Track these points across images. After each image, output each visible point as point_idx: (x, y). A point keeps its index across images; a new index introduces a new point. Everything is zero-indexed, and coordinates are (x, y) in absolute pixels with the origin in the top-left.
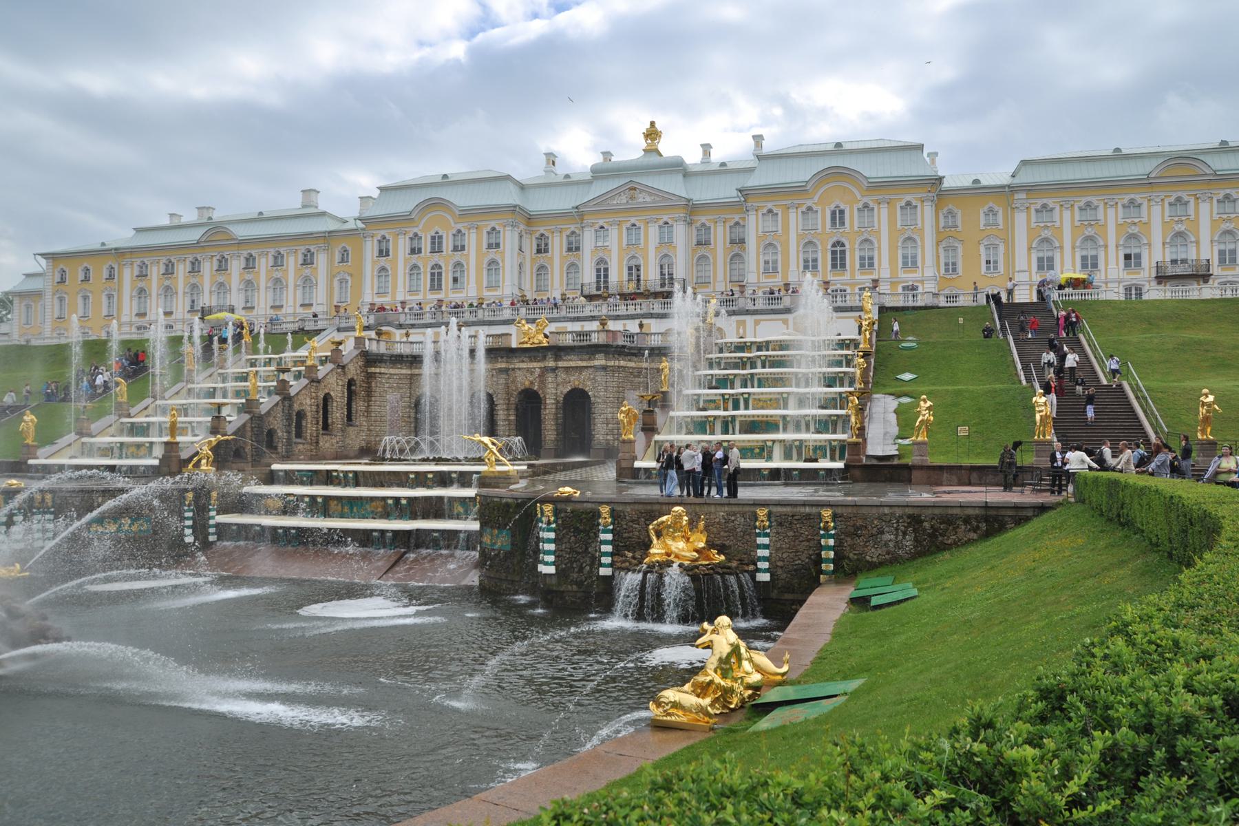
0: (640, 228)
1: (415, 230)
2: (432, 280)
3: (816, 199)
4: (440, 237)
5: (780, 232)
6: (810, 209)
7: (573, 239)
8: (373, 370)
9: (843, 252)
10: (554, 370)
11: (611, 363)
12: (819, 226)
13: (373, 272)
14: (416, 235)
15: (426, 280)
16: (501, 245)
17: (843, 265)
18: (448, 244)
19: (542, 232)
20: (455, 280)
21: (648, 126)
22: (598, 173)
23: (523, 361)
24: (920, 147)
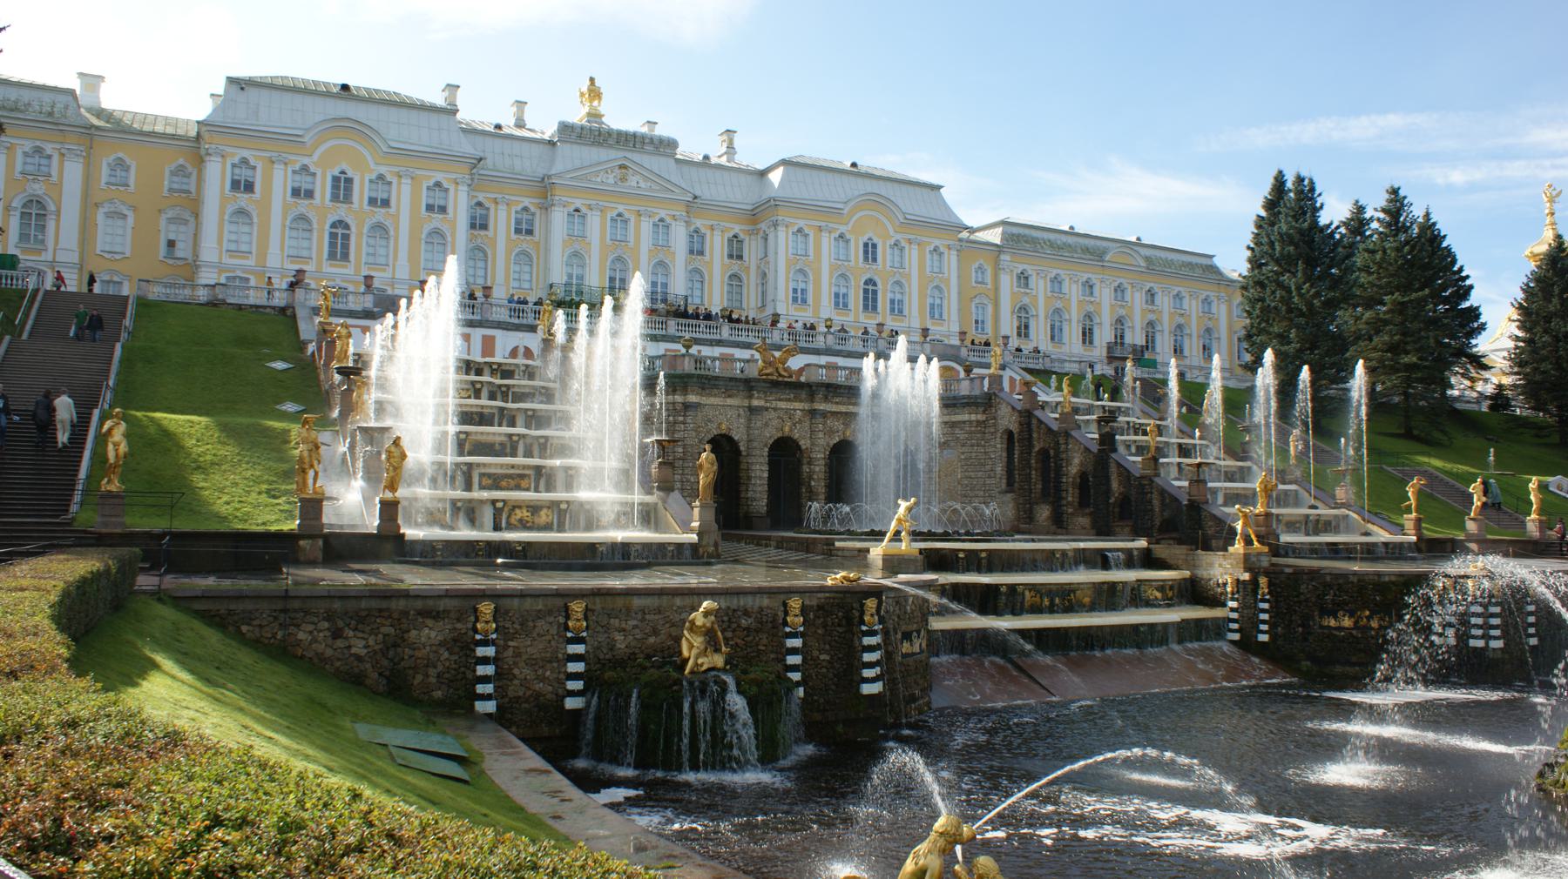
0: (626, 222)
1: (306, 161)
2: (332, 245)
4: (349, 181)
5: (811, 258)
6: (841, 236)
7: (525, 216)
9: (875, 292)
10: (824, 414)
12: (852, 258)
13: (222, 213)
14: (305, 168)
15: (320, 242)
16: (450, 209)
17: (875, 308)
18: (360, 192)
19: (481, 199)
21: (588, 83)
23: (780, 400)
24: (939, 187)
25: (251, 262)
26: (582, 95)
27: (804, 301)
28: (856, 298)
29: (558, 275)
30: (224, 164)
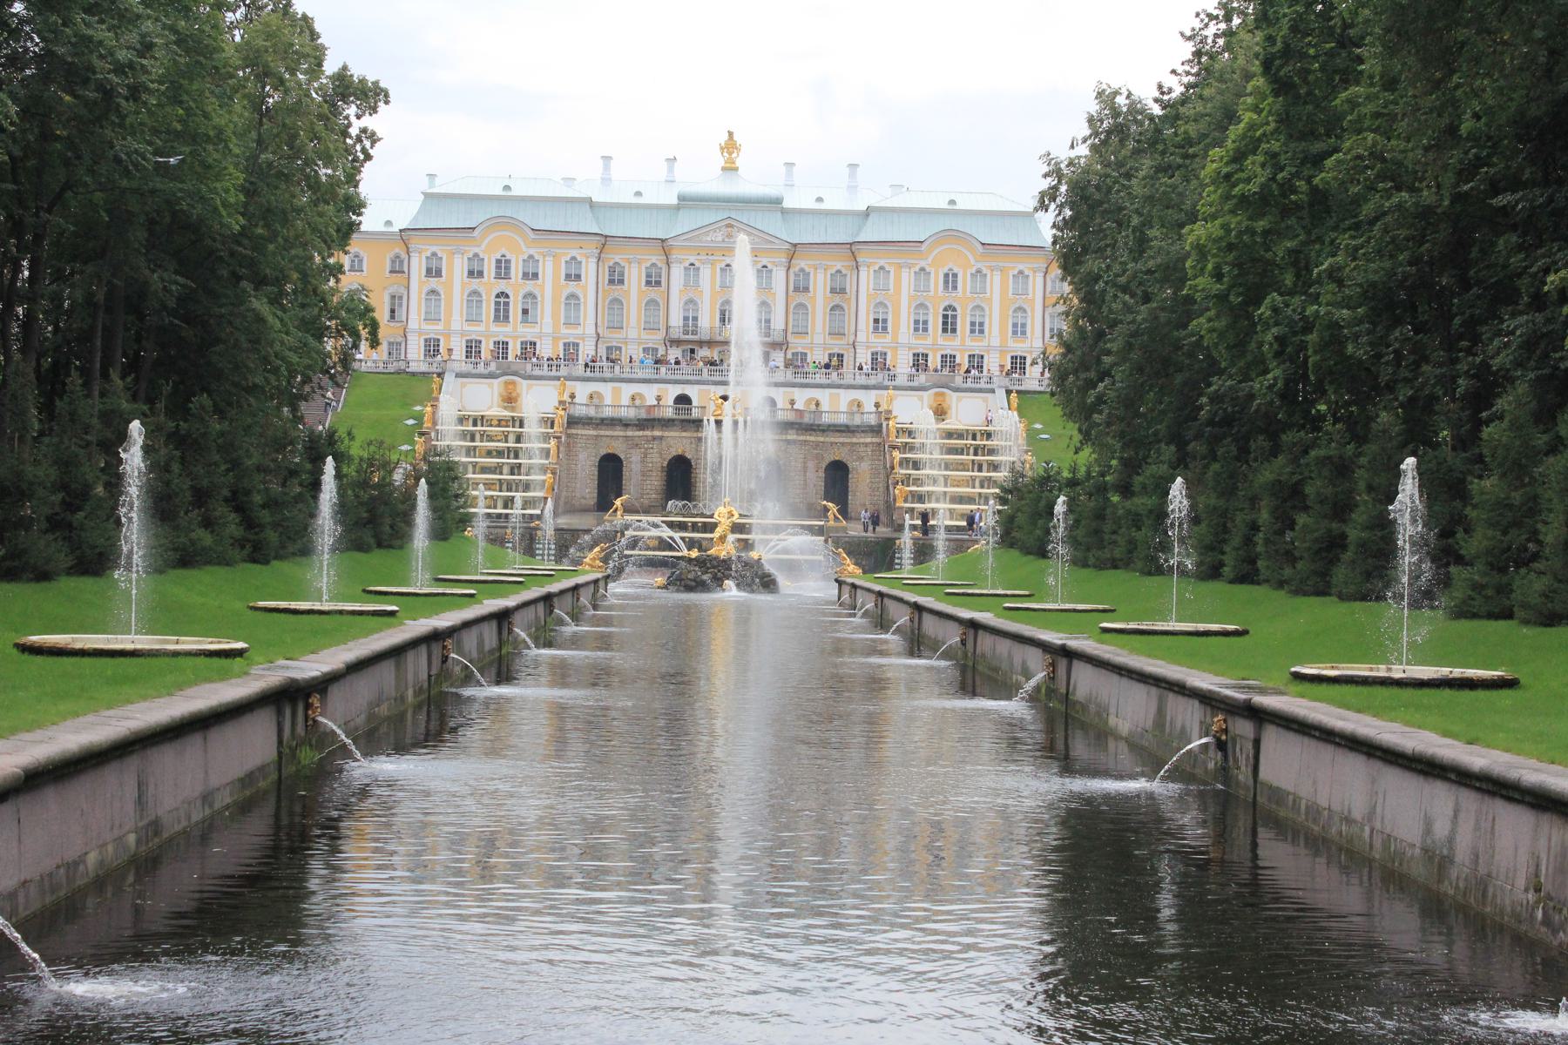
1: (476, 250)
2: (497, 310)
3: (930, 260)
4: (508, 262)
6: (922, 269)
8: (574, 431)
9: (954, 317)
11: (802, 438)
13: (420, 293)
14: (476, 255)
15: (488, 309)
17: (954, 331)
18: (516, 270)
20: (525, 312)
21: (726, 137)
22: (687, 202)
25: (440, 327)
26: (722, 149)
27: (885, 329)
28: (935, 323)
29: (676, 320)
30: (420, 257)
